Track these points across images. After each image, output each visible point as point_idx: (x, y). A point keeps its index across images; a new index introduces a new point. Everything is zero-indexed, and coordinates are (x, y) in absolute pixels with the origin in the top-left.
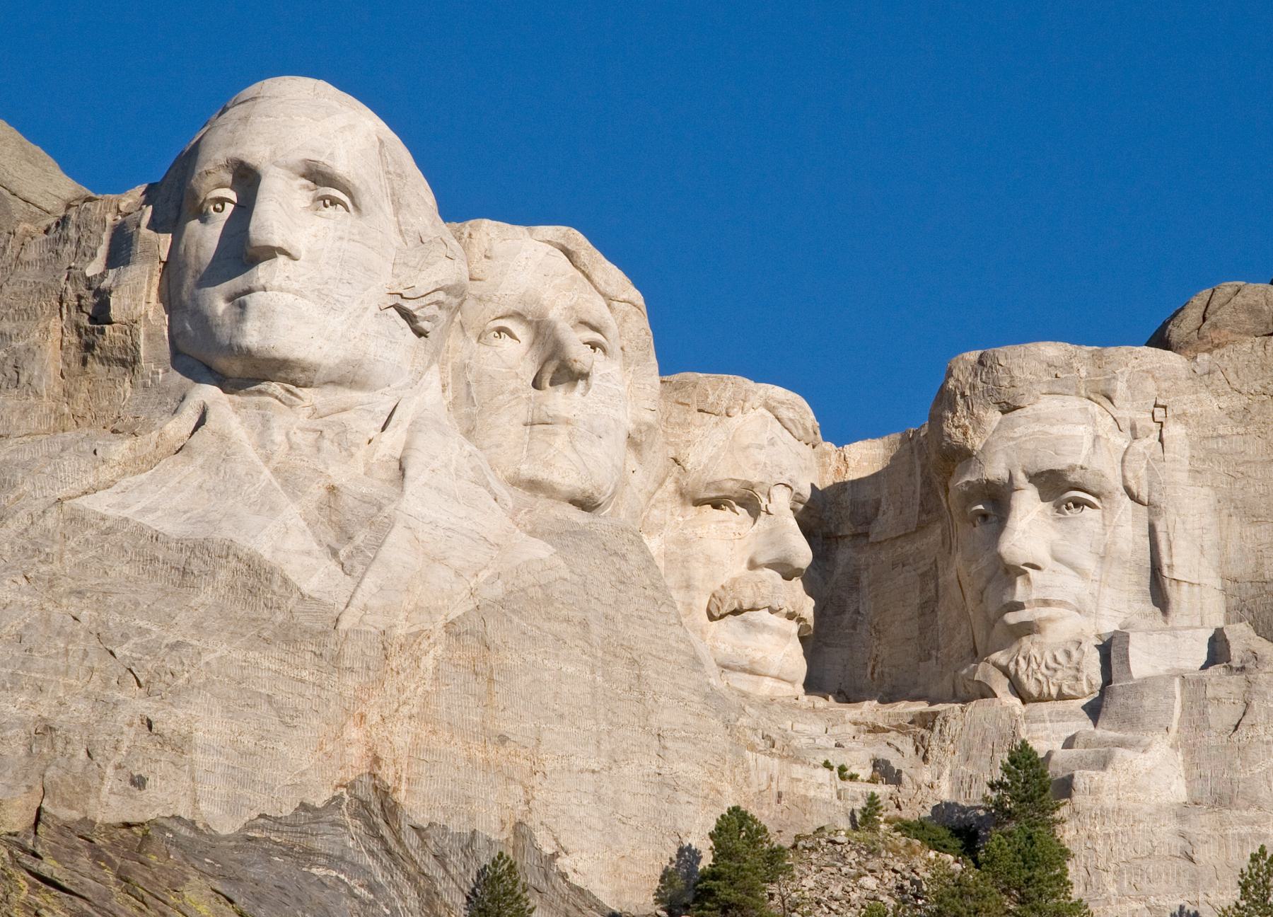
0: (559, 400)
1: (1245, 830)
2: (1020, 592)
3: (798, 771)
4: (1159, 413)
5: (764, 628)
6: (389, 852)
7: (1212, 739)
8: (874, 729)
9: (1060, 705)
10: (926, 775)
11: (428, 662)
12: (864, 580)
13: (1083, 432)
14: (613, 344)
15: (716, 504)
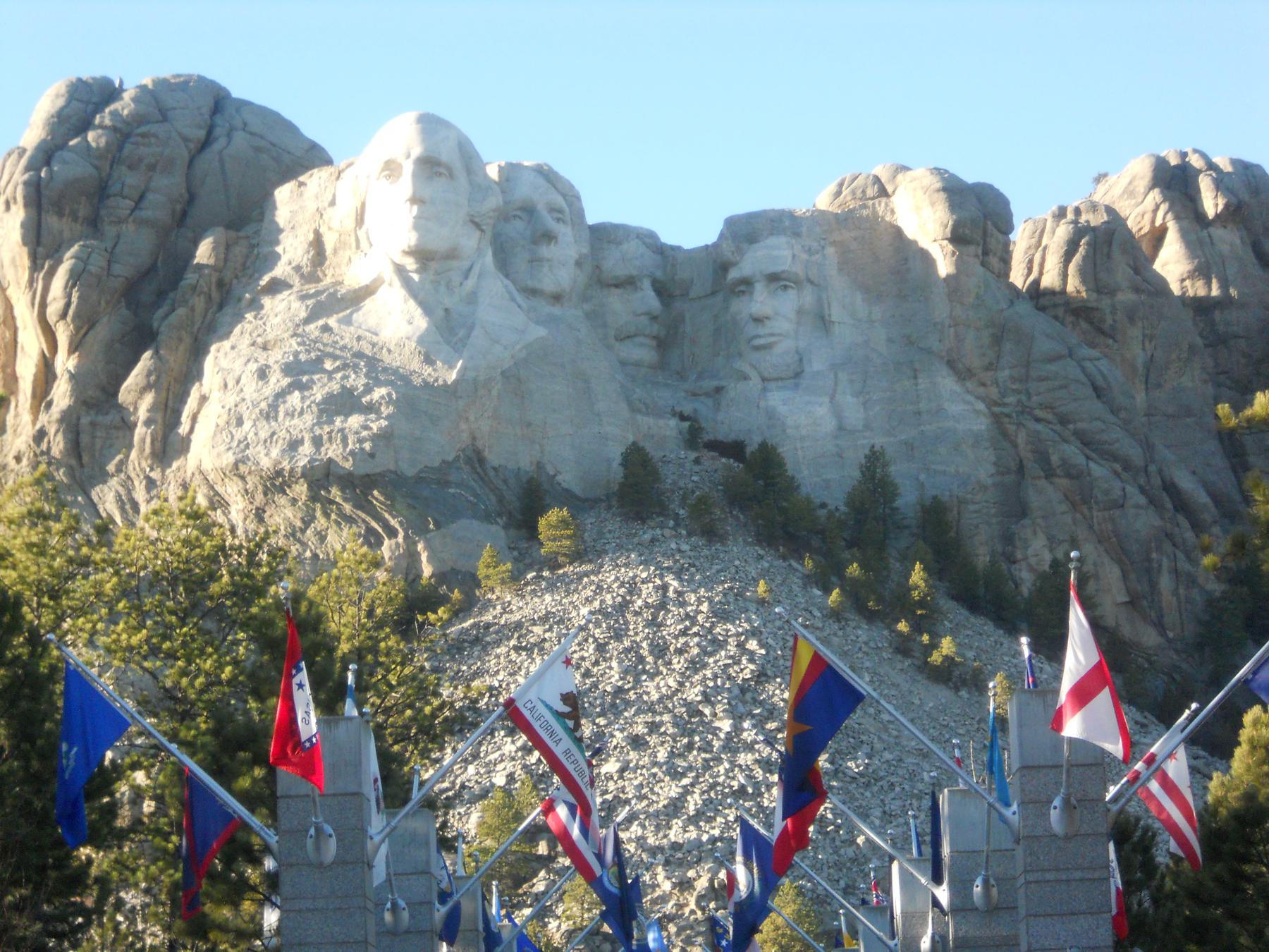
0: (545, 251)
1: (865, 442)
2: (761, 331)
3: (661, 422)
4: (822, 242)
5: (642, 345)
6: (482, 479)
7: (849, 399)
8: (694, 395)
9: (780, 384)
10: (721, 416)
11: (494, 392)
12: (687, 316)
13: (787, 253)
14: (568, 219)
15: (617, 286)
